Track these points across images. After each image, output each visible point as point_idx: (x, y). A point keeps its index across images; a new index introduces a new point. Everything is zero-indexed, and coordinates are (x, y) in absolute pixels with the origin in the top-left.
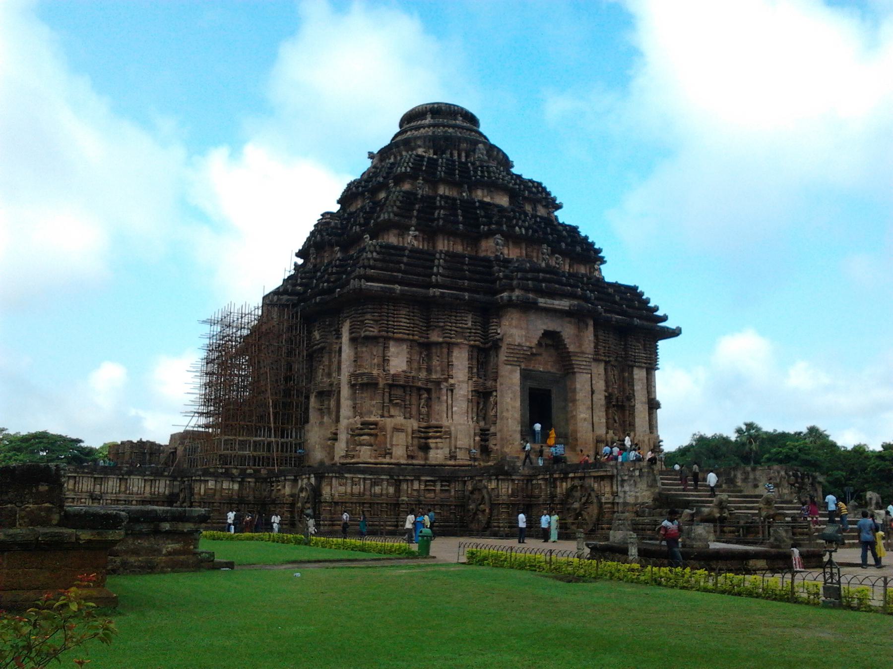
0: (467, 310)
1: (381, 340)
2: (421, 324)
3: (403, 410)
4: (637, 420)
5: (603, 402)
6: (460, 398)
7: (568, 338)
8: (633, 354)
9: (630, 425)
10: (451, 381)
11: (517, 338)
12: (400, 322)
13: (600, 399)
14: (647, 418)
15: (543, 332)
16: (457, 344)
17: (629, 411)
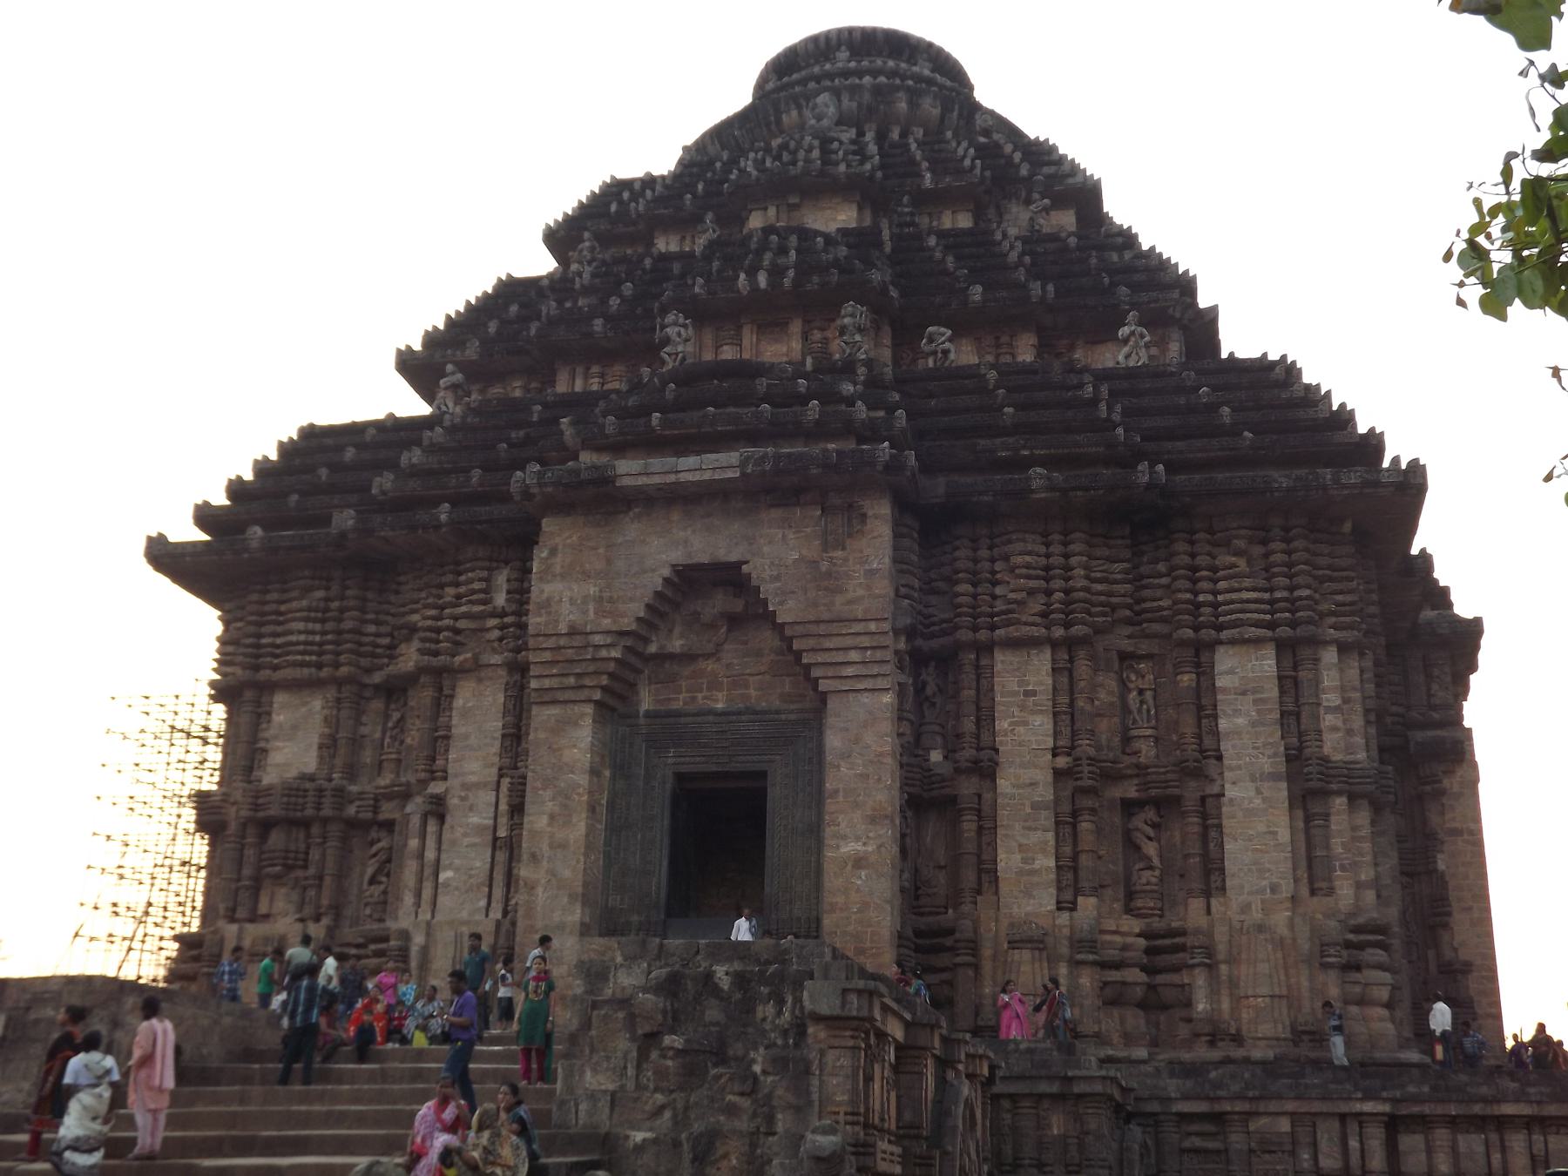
0: (490, 560)
1: (249, 694)
2: (372, 629)
3: (295, 896)
4: (1227, 847)
5: (1045, 793)
6: (466, 841)
7: (777, 578)
8: (1201, 598)
9: (1207, 873)
10: (436, 788)
11: (565, 608)
12: (291, 633)
13: (1031, 784)
14: (1284, 835)
15: (666, 572)
16: (463, 671)
17: (1204, 816)
